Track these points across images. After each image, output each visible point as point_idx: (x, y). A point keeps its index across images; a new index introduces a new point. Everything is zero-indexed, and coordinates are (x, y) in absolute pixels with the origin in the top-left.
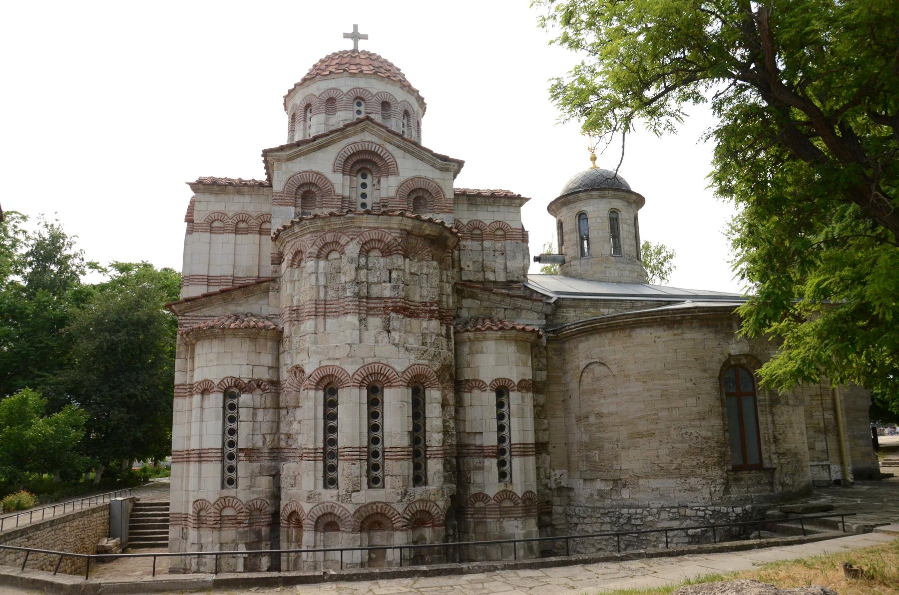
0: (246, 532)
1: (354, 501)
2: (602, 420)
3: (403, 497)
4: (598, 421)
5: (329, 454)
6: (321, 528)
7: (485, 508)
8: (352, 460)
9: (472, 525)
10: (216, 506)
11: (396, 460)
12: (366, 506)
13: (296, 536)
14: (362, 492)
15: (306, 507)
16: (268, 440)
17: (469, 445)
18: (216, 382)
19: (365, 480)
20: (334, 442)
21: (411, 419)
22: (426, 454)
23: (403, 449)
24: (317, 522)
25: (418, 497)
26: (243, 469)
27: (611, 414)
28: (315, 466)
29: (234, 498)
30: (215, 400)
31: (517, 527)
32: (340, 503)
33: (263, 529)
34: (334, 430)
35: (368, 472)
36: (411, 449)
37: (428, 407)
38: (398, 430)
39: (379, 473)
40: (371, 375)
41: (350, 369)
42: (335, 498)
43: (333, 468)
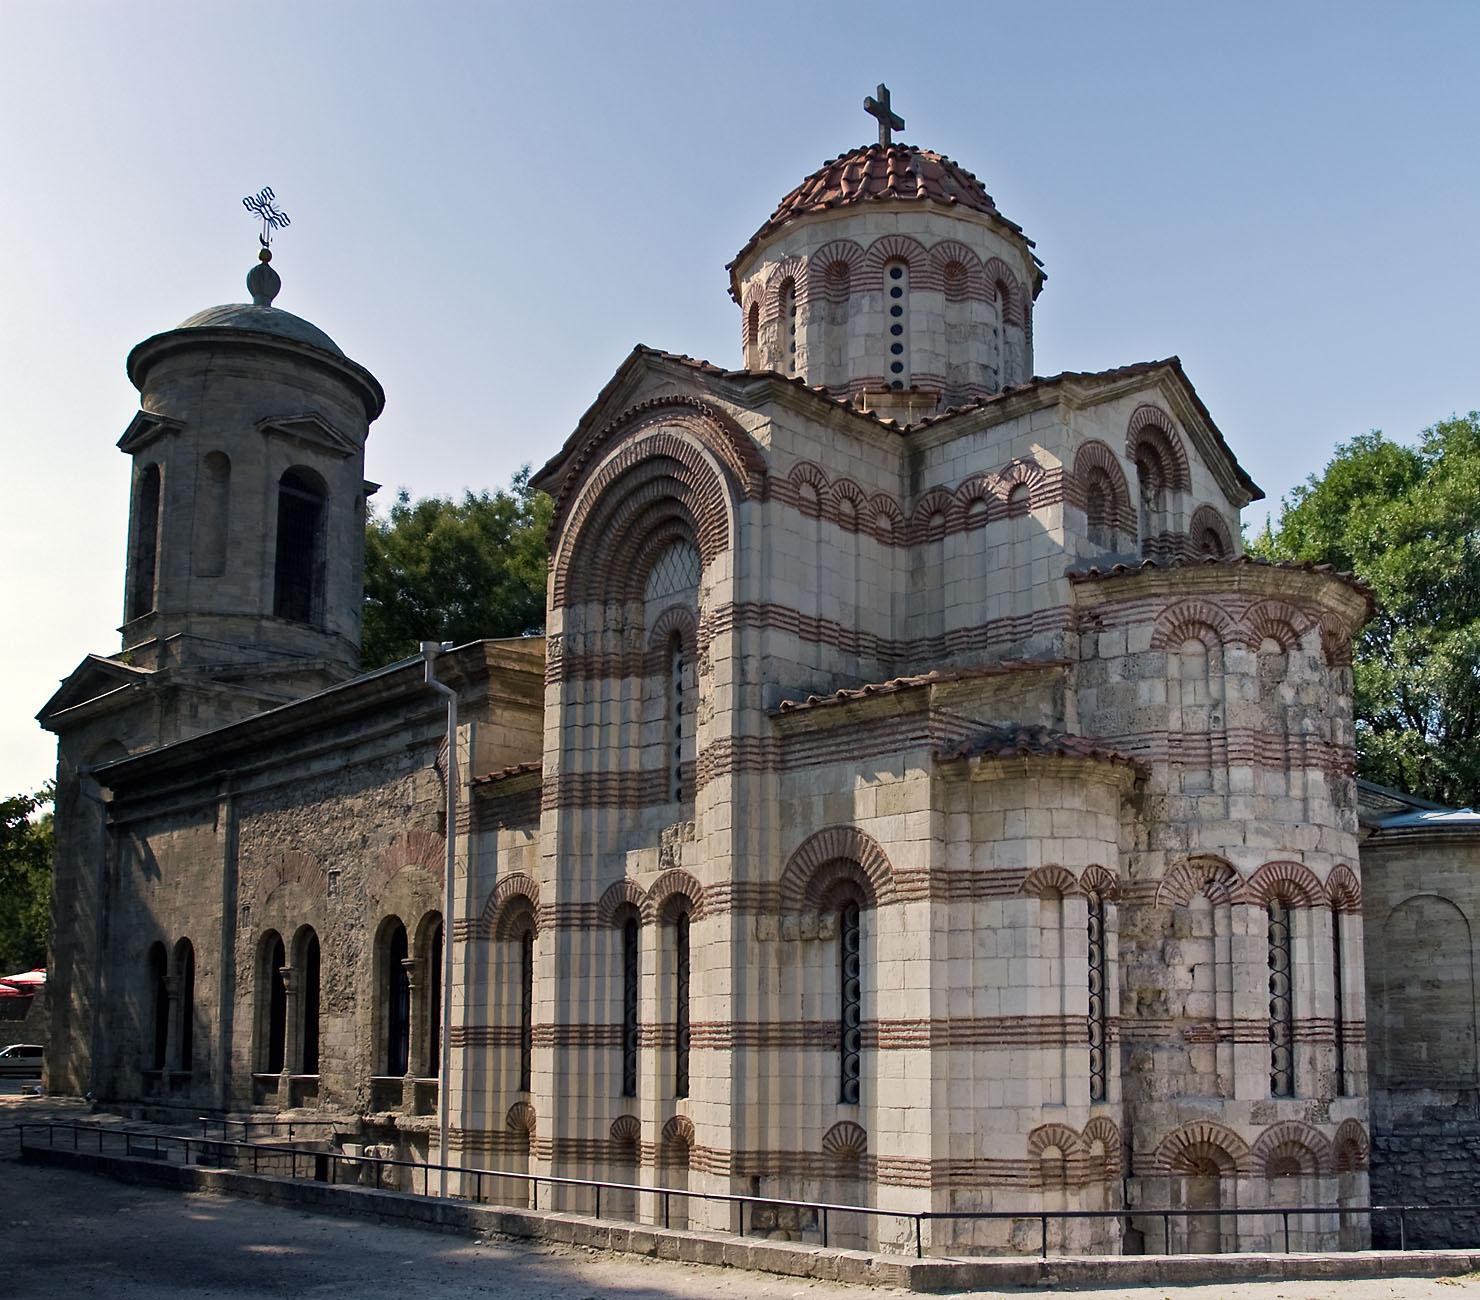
2: (1437, 992)
4: (1428, 993)
5: (1284, 1031)
10: (1085, 1137)
13: (1188, 1193)
15: (1250, 1134)
18: (1079, 876)
27: (1455, 984)
30: (1076, 910)
32: (1310, 1123)
41: (1322, 869)
42: (1303, 1114)
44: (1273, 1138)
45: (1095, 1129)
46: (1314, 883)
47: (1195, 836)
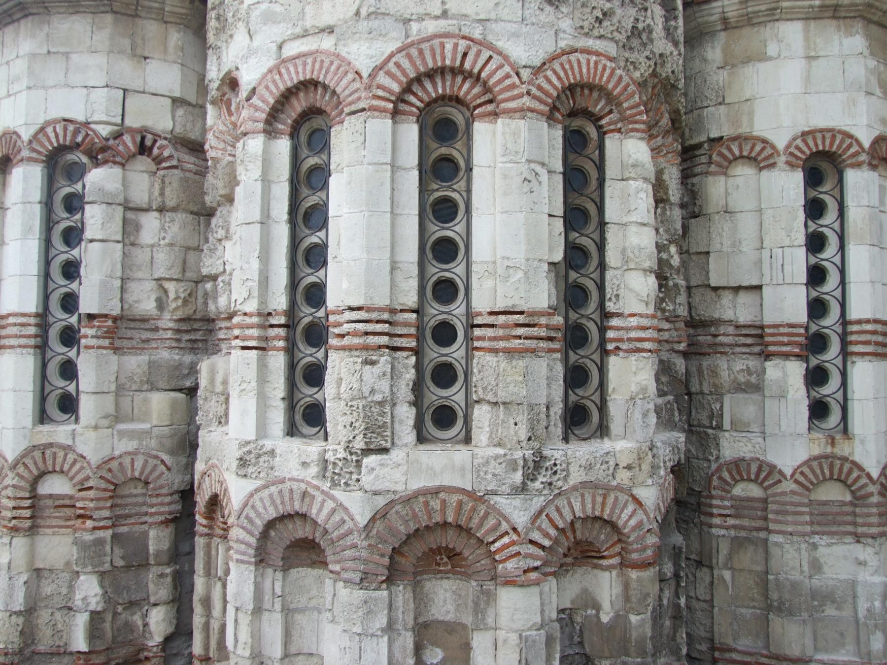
0: (100, 542)
1: (367, 480)
3: (529, 477)
5: (304, 330)
6: (276, 554)
7: (765, 501)
8: (366, 348)
9: (724, 549)
10: (21, 469)
11: (508, 351)
12: (409, 500)
14: (397, 455)
15: (237, 491)
16: (172, 295)
17: (718, 322)
19: (406, 414)
20: (316, 295)
21: (559, 225)
22: (603, 341)
23: (528, 319)
24: (264, 535)
25: (577, 476)
26: (92, 369)
28: (262, 367)
29: (68, 449)
31: (862, 563)
32: (326, 486)
33: (152, 533)
34: (316, 256)
35: (417, 388)
36: (559, 320)
37: (612, 190)
38: (519, 254)
39: (455, 395)
40: (430, 75)
42: (314, 470)
43: (315, 375)
44: (268, 504)
45: (39, 463)
46: (350, 76)
47: (224, 54)
